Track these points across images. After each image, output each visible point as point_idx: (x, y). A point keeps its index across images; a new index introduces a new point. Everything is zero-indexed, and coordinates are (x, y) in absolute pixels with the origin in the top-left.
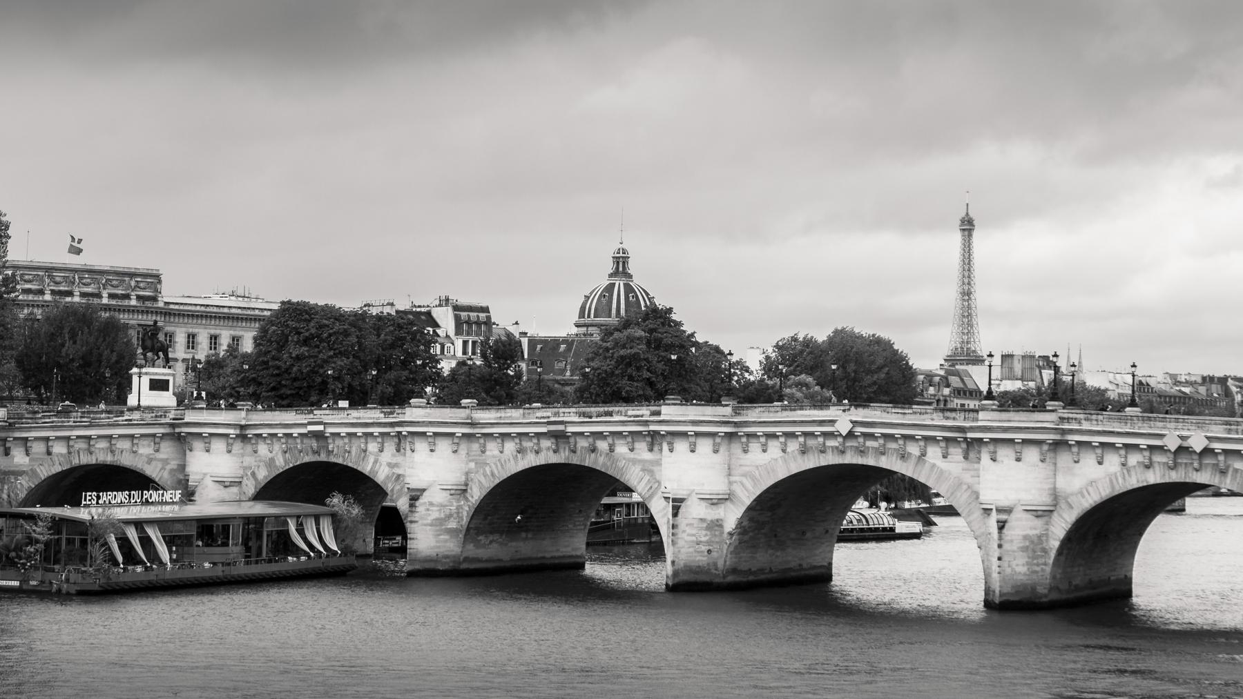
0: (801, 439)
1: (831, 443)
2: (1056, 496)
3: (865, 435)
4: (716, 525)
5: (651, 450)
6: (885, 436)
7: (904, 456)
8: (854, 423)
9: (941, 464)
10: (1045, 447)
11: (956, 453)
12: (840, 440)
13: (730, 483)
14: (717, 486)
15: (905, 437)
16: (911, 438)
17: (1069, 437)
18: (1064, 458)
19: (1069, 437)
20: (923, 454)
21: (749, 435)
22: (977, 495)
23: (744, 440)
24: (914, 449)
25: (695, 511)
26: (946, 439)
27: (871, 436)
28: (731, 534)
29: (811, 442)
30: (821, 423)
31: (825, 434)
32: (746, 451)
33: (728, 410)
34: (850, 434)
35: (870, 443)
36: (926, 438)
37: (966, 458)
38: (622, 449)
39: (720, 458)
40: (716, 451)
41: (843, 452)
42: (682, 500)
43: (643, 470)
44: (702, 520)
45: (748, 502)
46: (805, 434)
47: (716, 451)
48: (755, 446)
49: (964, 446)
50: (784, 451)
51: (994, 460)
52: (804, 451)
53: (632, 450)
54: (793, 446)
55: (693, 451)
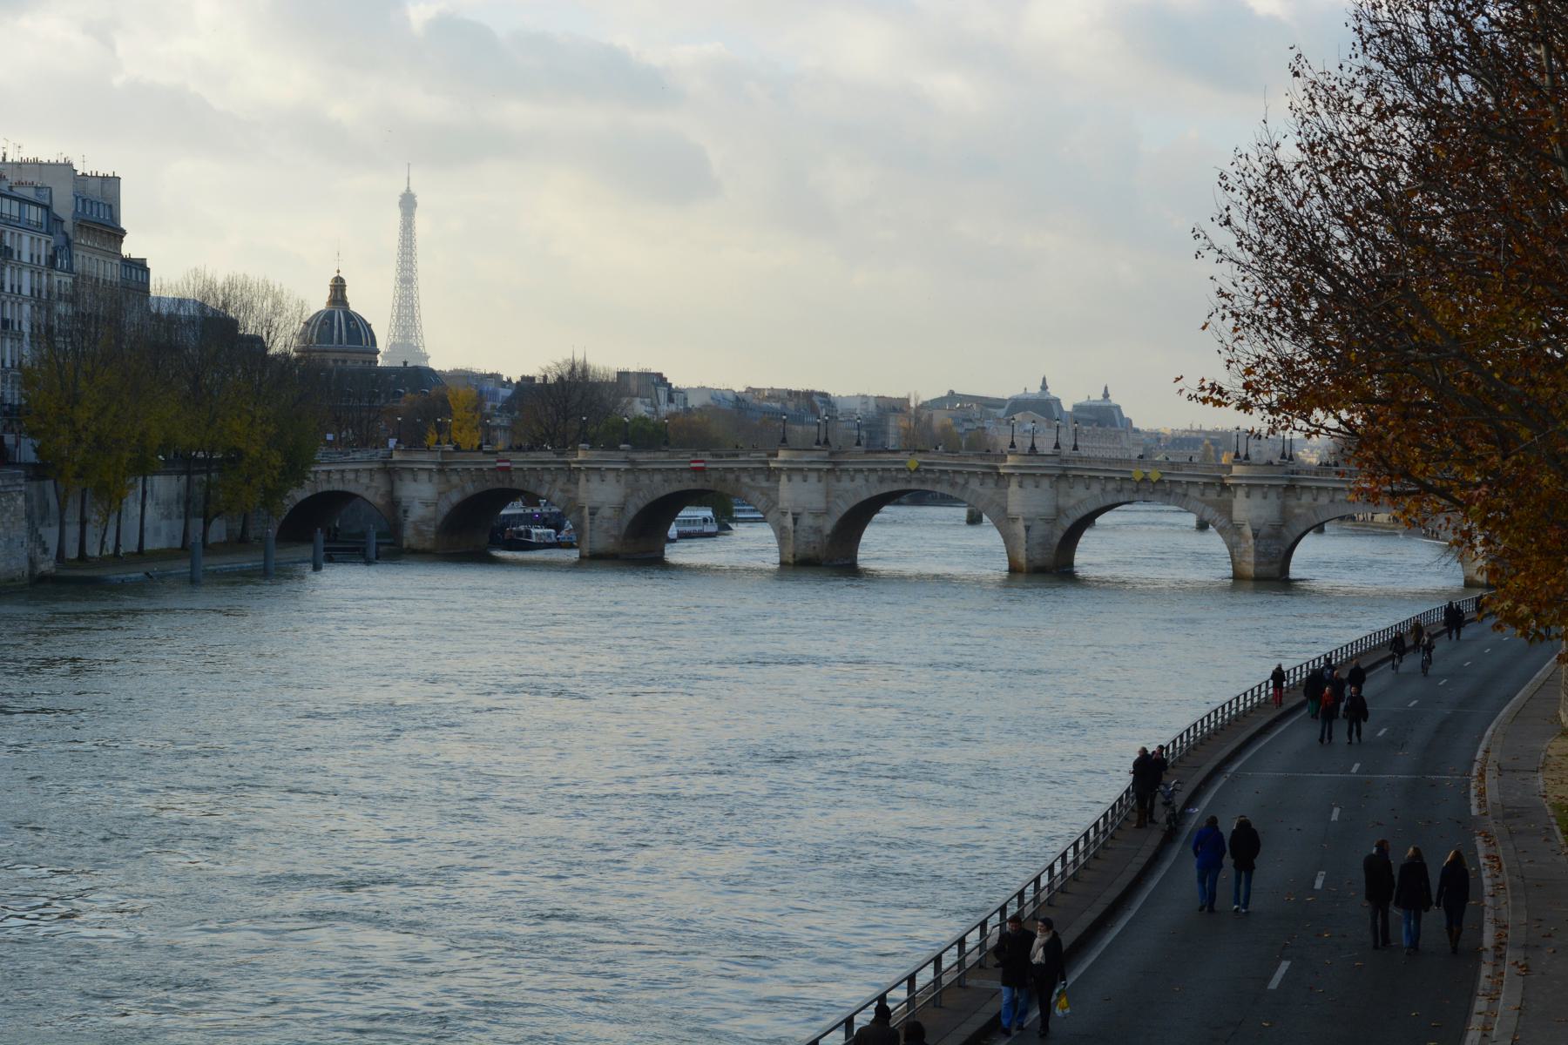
0: (880, 473)
1: (901, 476)
2: (1060, 511)
3: (926, 471)
4: (818, 530)
5: (768, 480)
6: (941, 471)
7: (953, 484)
8: (921, 463)
9: (980, 490)
10: (1054, 479)
11: (990, 482)
12: (909, 473)
13: (828, 502)
14: (818, 502)
15: (954, 472)
16: (960, 472)
17: (1069, 472)
18: (1063, 485)
19: (1069, 472)
20: (967, 483)
21: (842, 470)
22: (1005, 510)
23: (838, 473)
24: (960, 480)
25: (807, 521)
26: (983, 473)
27: (932, 471)
28: (827, 536)
29: (887, 474)
30: (896, 463)
31: (897, 470)
32: (839, 480)
33: (826, 454)
34: (917, 470)
35: (928, 476)
36: (969, 473)
37: (996, 485)
38: (745, 479)
39: (821, 486)
40: (819, 481)
41: (909, 482)
42: (799, 514)
43: (762, 494)
44: (811, 527)
45: (840, 515)
46: (883, 470)
47: (819, 481)
48: (845, 478)
49: (996, 477)
50: (867, 481)
51: (1020, 486)
52: (881, 480)
53: (753, 480)
54: (873, 478)
55: (805, 481)
